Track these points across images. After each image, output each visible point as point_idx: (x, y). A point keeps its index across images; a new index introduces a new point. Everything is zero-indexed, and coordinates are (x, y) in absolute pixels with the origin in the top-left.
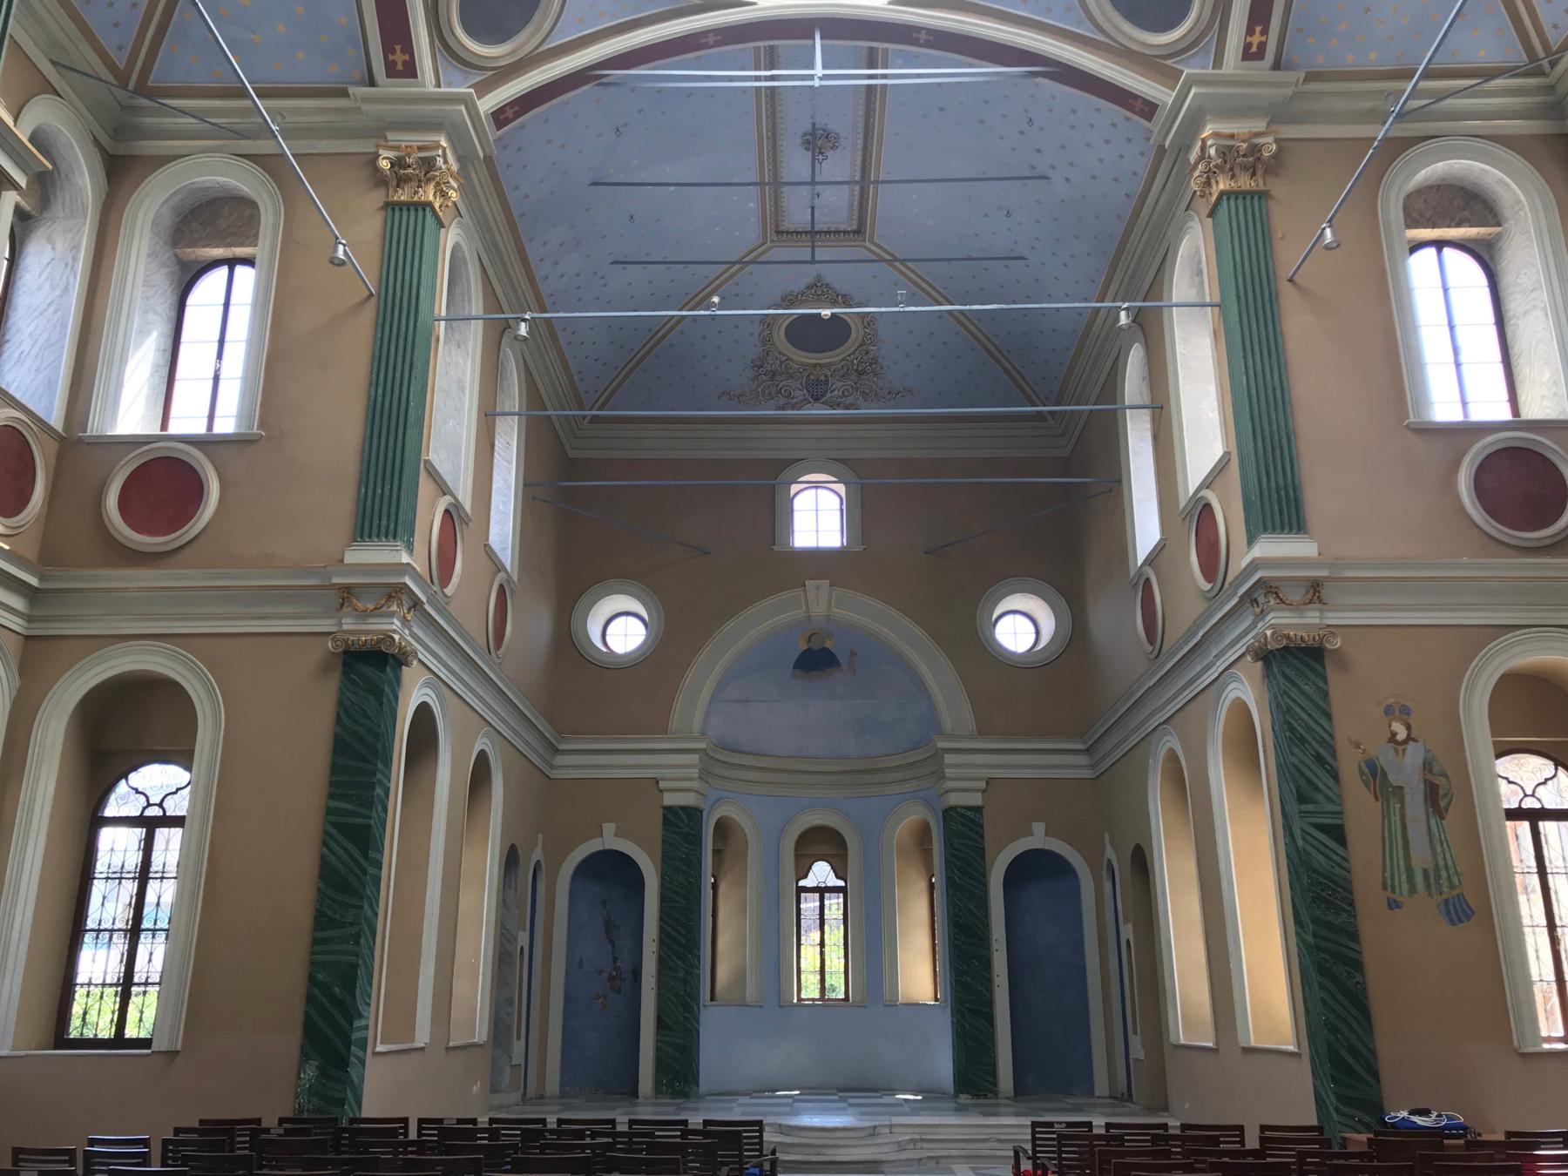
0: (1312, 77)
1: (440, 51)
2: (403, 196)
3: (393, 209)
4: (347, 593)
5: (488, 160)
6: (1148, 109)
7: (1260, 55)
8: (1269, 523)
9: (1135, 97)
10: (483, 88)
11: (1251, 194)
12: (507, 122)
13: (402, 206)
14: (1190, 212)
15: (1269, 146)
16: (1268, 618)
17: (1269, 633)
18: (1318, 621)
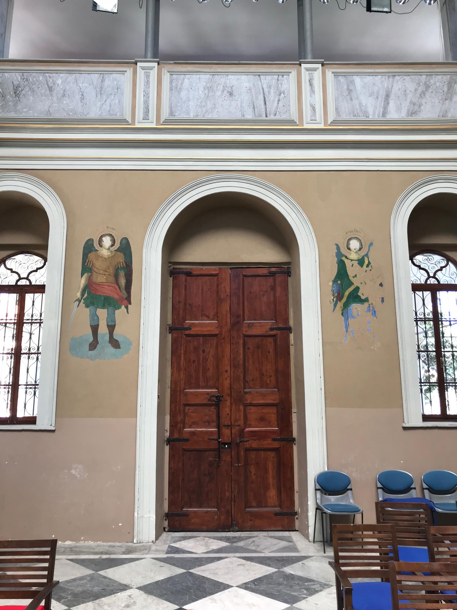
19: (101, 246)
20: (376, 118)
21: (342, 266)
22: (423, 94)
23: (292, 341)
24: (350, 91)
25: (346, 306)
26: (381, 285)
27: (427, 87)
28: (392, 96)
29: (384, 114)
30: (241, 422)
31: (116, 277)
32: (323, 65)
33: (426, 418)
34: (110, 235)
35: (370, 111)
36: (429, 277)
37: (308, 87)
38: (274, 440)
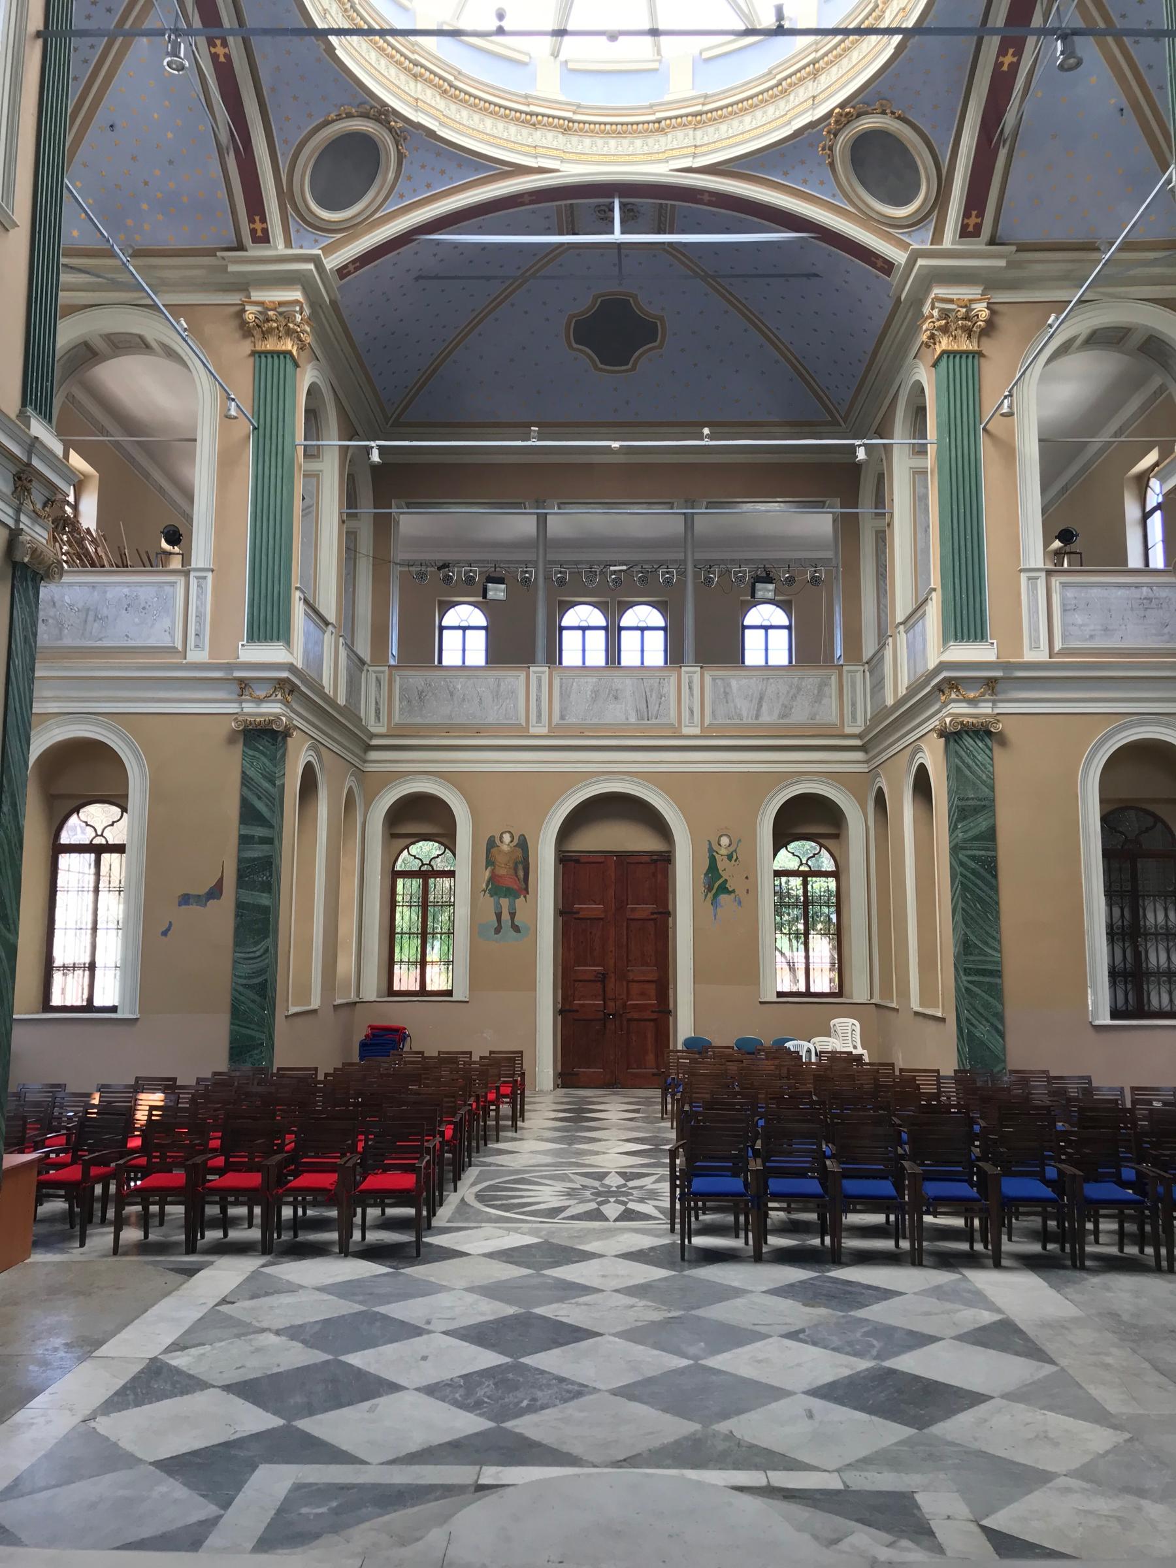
0: (1022, 248)
1: (294, 219)
2: (270, 345)
3: (260, 357)
4: (244, 685)
5: (333, 303)
6: (887, 266)
7: (976, 233)
8: (959, 635)
9: (877, 256)
10: (329, 250)
11: (967, 353)
12: (349, 273)
13: (266, 353)
14: (916, 360)
15: (981, 310)
16: (949, 707)
17: (948, 720)
18: (989, 711)
19: (502, 842)
20: (750, 721)
21: (713, 860)
22: (794, 697)
23: (671, 925)
24: (726, 693)
25: (715, 896)
26: (747, 878)
27: (799, 689)
28: (766, 698)
29: (757, 718)
30: (624, 997)
31: (516, 869)
32: (702, 667)
33: (780, 994)
34: (510, 832)
35: (744, 714)
36: (801, 864)
37: (688, 690)
38: (653, 1012)
